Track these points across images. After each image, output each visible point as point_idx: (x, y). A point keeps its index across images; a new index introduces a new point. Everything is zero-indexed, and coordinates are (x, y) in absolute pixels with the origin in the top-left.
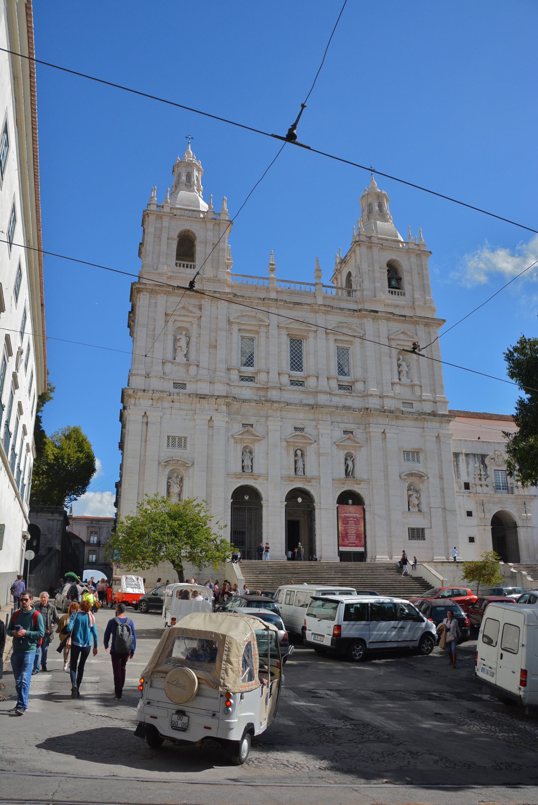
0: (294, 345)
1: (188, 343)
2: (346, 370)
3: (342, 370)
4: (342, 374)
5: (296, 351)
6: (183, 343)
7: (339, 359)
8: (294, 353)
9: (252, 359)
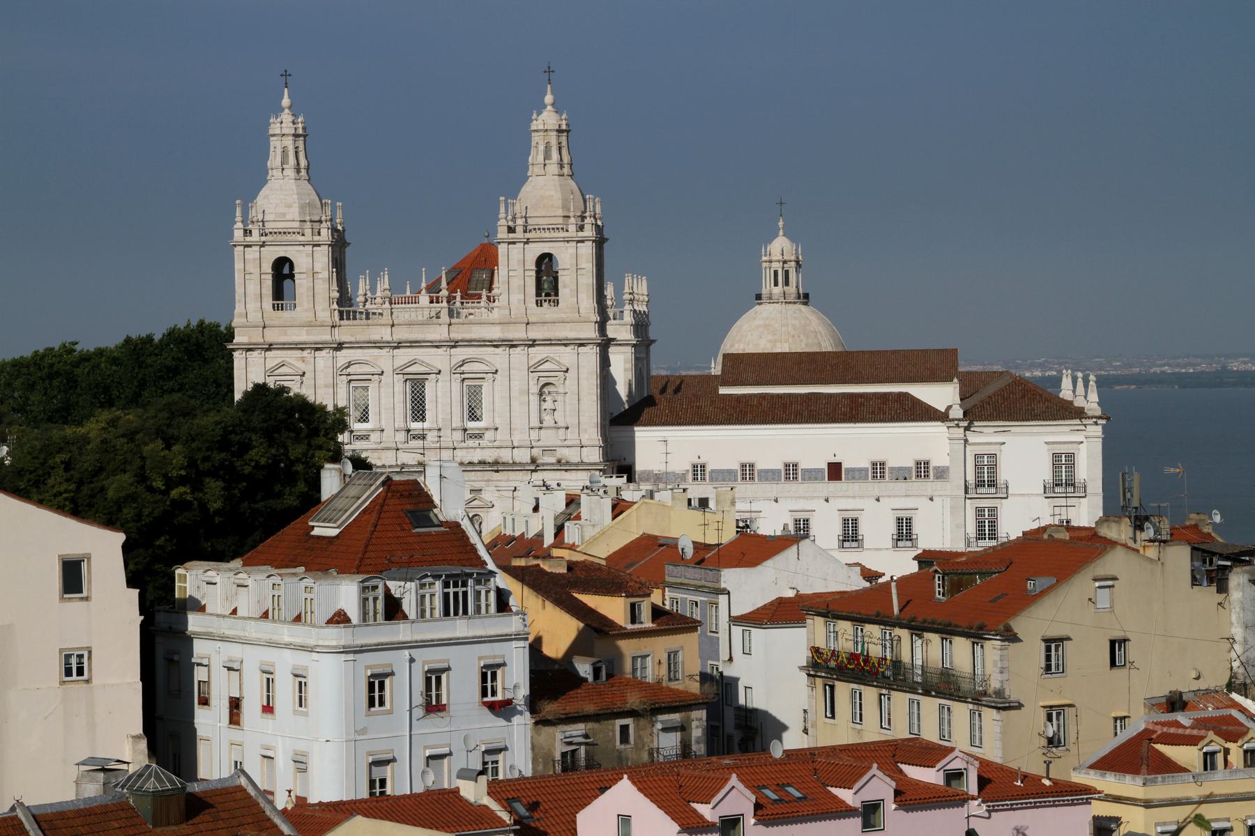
0: (415, 389)
2: (478, 413)
3: (473, 414)
4: (473, 419)
5: (418, 397)
7: (470, 401)
8: (416, 399)
9: (367, 413)
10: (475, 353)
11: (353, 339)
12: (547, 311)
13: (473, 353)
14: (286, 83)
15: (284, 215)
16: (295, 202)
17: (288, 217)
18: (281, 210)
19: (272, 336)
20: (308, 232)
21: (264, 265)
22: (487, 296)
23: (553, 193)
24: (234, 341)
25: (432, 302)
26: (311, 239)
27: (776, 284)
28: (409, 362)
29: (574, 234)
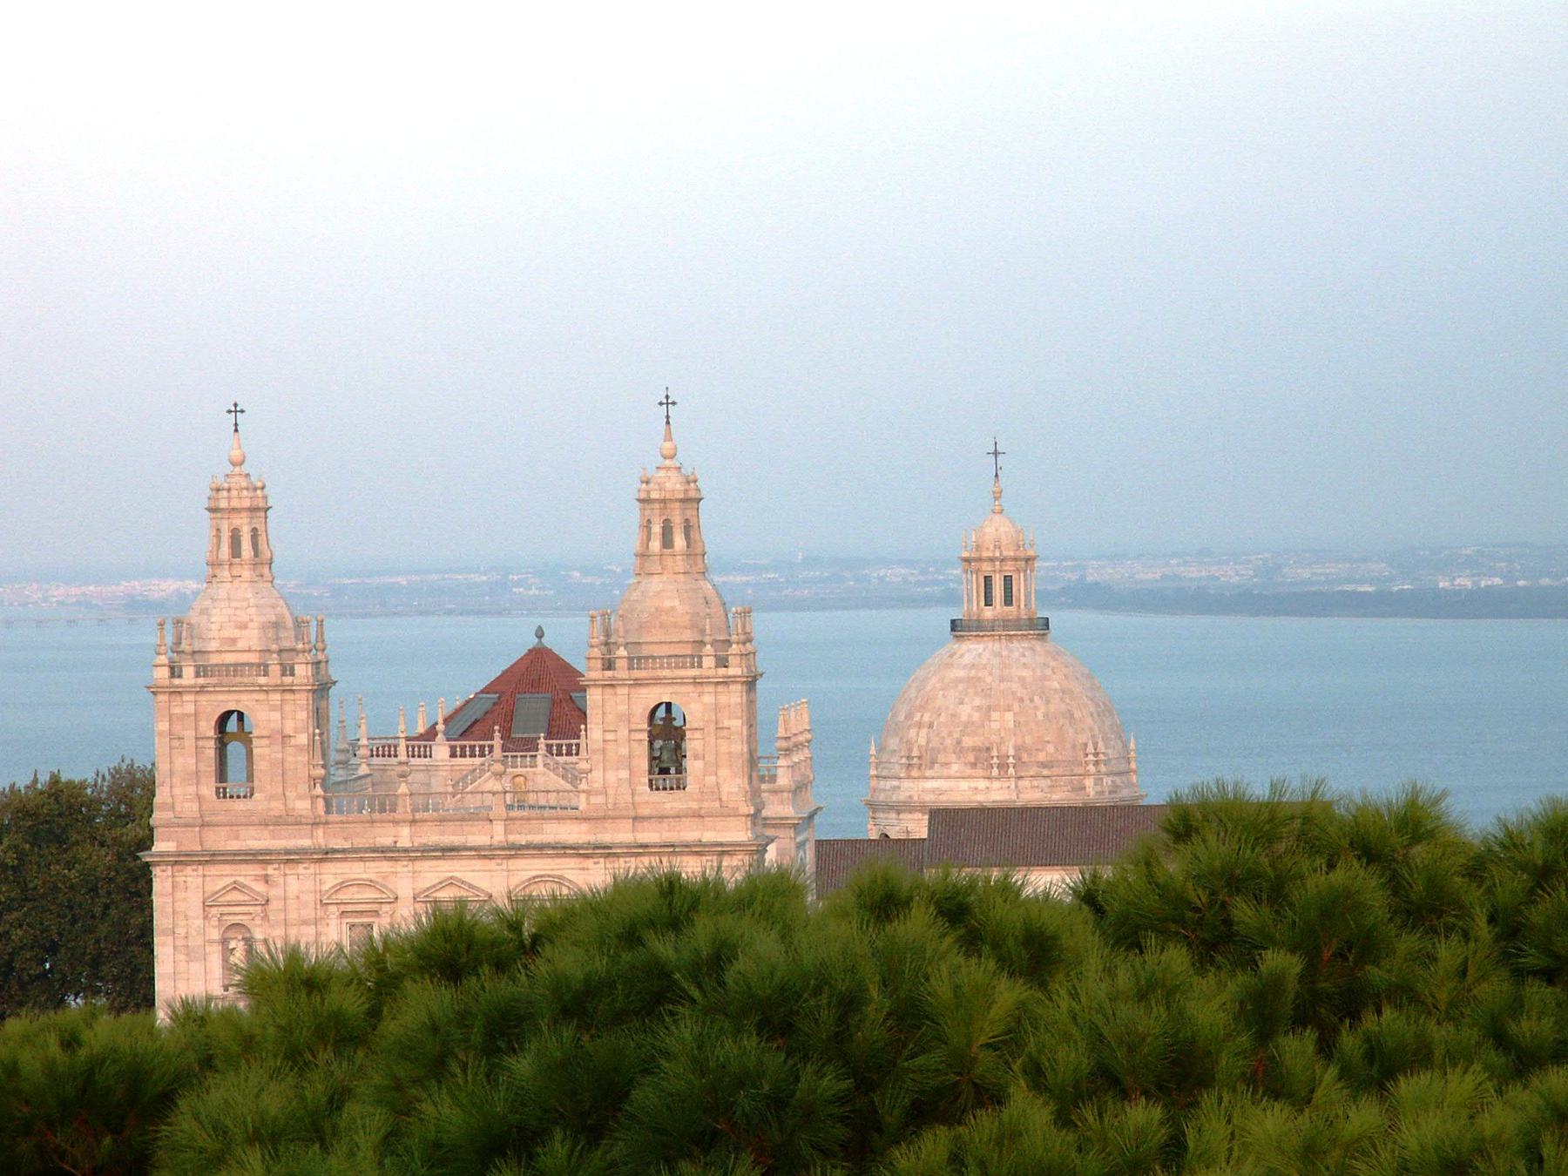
10: (550, 867)
11: (347, 845)
12: (670, 802)
13: (546, 867)
15: (234, 641)
16: (252, 620)
17: (241, 645)
18: (226, 634)
19: (218, 840)
20: (275, 670)
21: (203, 724)
22: (547, 745)
23: (676, 603)
24: (153, 849)
25: (453, 755)
26: (279, 682)
27: (988, 602)
28: (441, 883)
29: (712, 672)
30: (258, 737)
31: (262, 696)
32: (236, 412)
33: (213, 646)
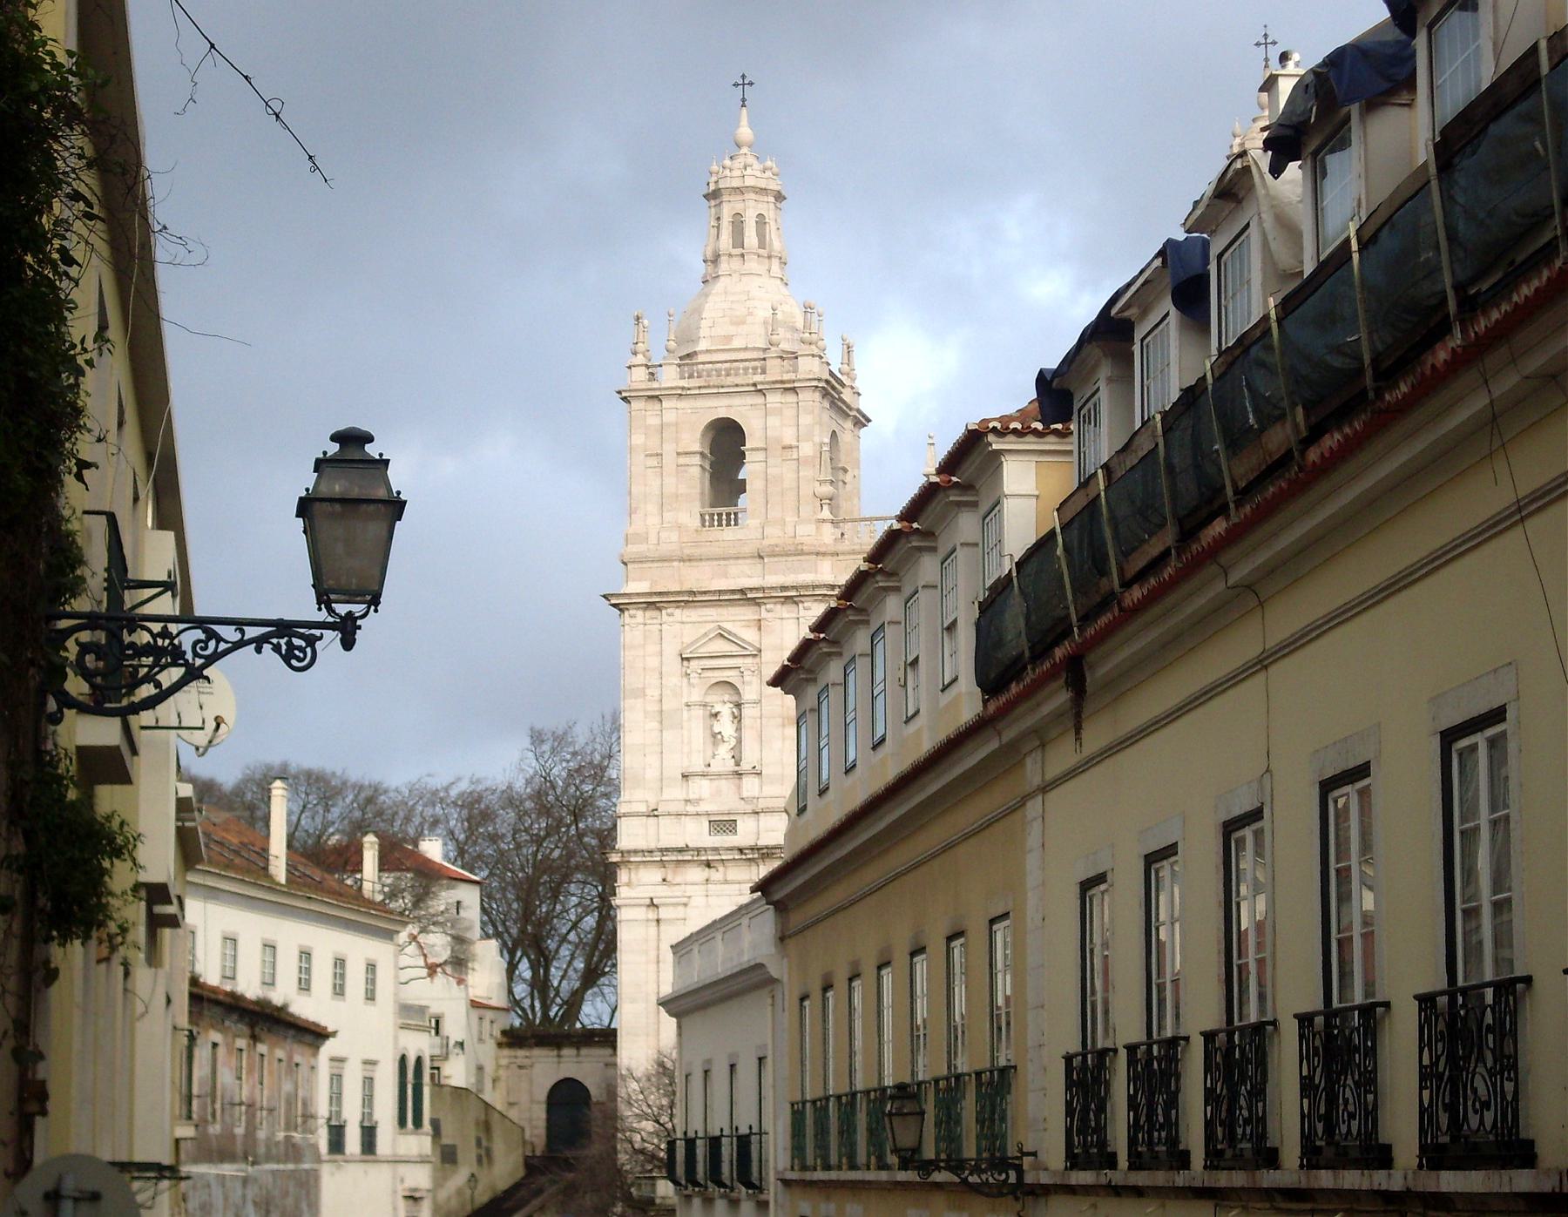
1: (738, 718)
6: (726, 726)
14: (744, 100)
15: (729, 338)
17: (736, 344)
18: (720, 331)
30: (752, 450)
31: (759, 400)
32: (744, 84)
33: (702, 345)
